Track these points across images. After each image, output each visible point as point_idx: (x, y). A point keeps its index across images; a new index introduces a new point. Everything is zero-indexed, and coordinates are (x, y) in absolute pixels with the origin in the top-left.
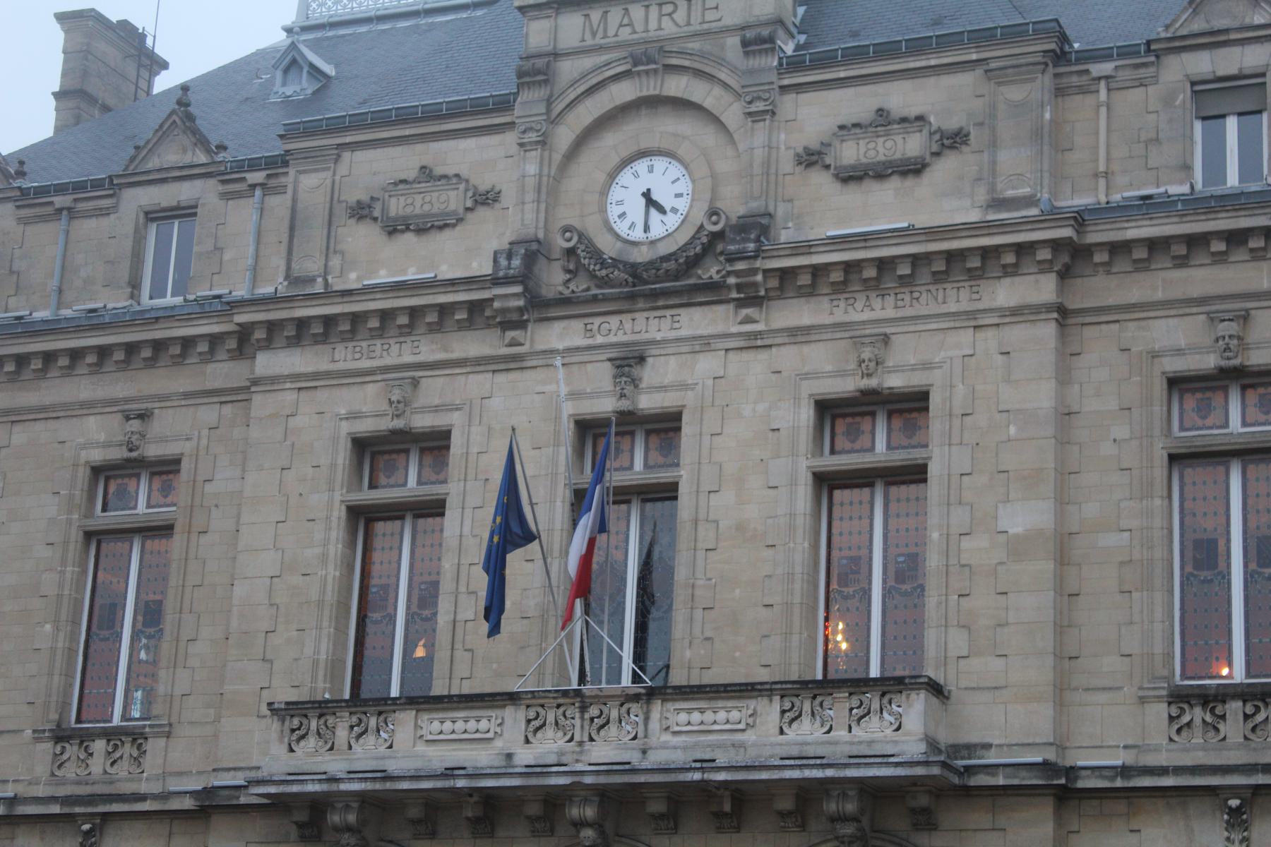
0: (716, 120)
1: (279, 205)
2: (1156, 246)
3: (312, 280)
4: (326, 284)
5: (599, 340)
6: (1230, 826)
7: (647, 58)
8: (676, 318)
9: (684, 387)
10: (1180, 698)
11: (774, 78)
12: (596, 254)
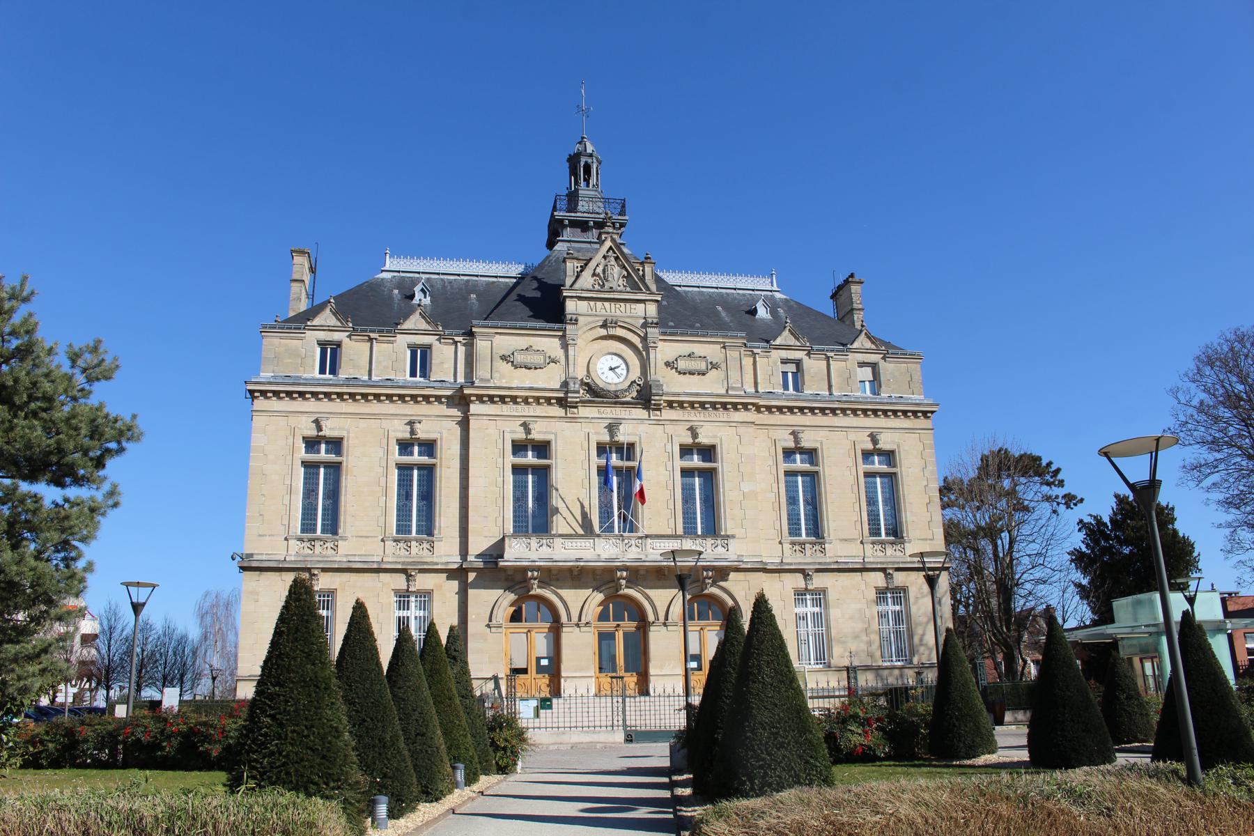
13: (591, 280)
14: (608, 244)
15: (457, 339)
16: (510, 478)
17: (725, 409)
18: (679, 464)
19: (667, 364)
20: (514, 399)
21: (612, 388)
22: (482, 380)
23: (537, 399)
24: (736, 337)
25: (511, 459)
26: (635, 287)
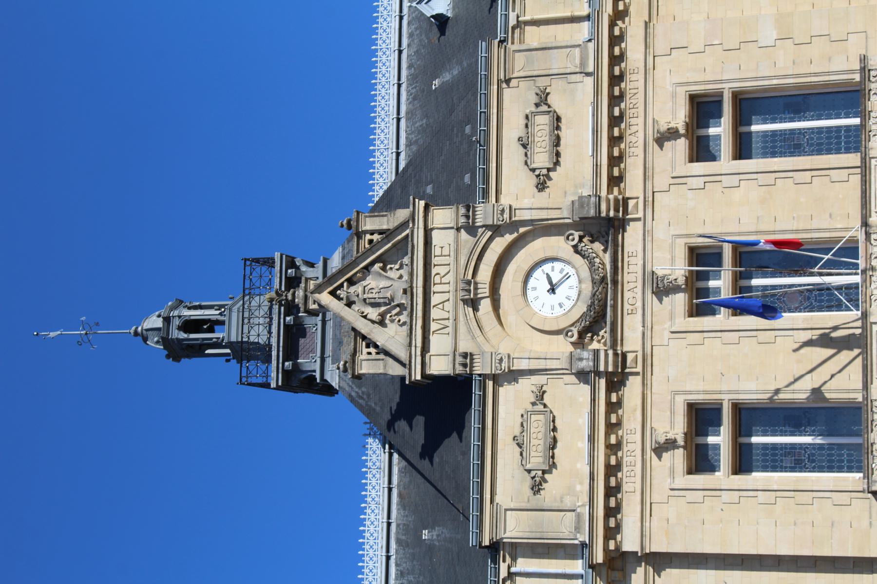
3: (579, 516)
4: (583, 505)
5: (639, 304)
8: (630, 254)
9: (672, 246)
11: (489, 206)
13: (392, 329)
14: (325, 298)
15: (503, 573)
16: (758, 478)
17: (621, 78)
18: (726, 163)
19: (541, 186)
20: (612, 470)
21: (588, 288)
22: (578, 529)
23: (611, 428)
24: (488, 60)
25: (723, 477)
26: (403, 248)
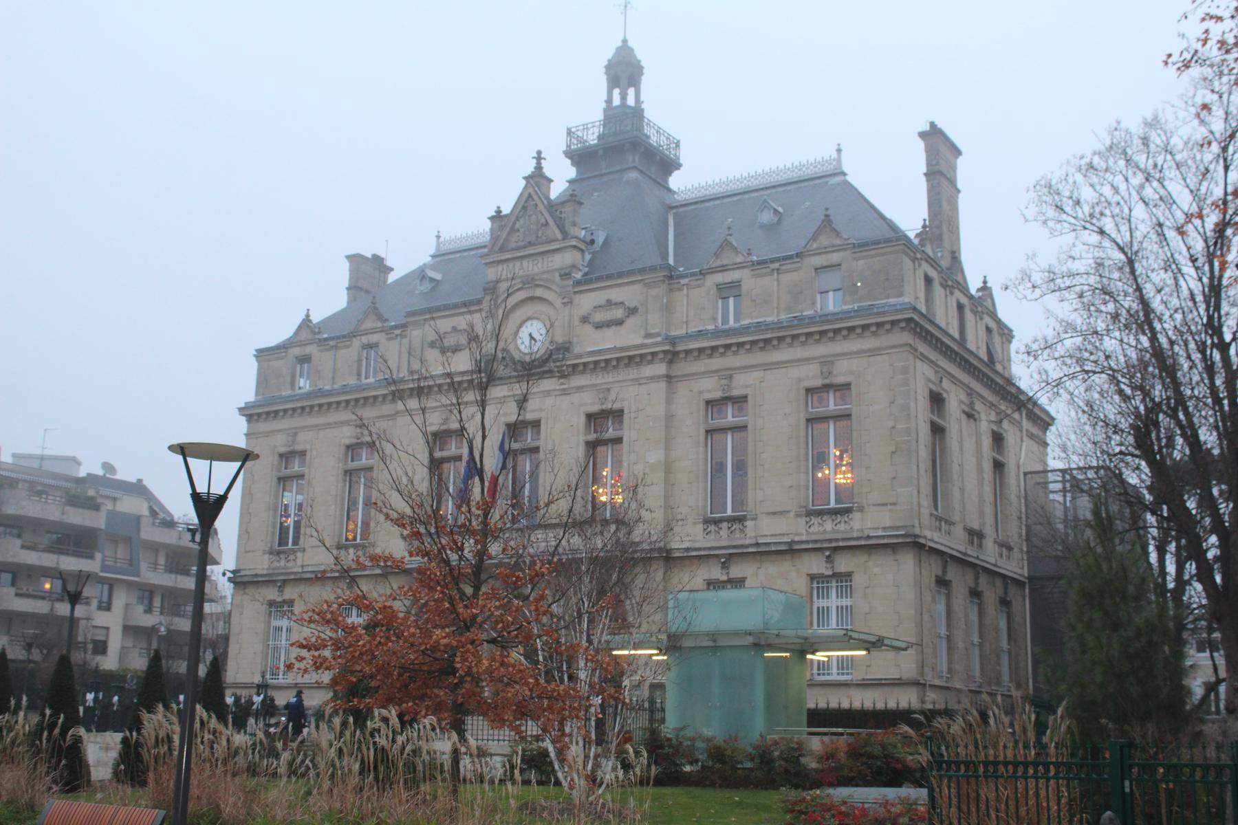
0: (551, 304)
1: (406, 341)
2: (701, 351)
6: (722, 568)
7: (530, 282)
9: (541, 410)
10: (707, 521)
12: (513, 359)
